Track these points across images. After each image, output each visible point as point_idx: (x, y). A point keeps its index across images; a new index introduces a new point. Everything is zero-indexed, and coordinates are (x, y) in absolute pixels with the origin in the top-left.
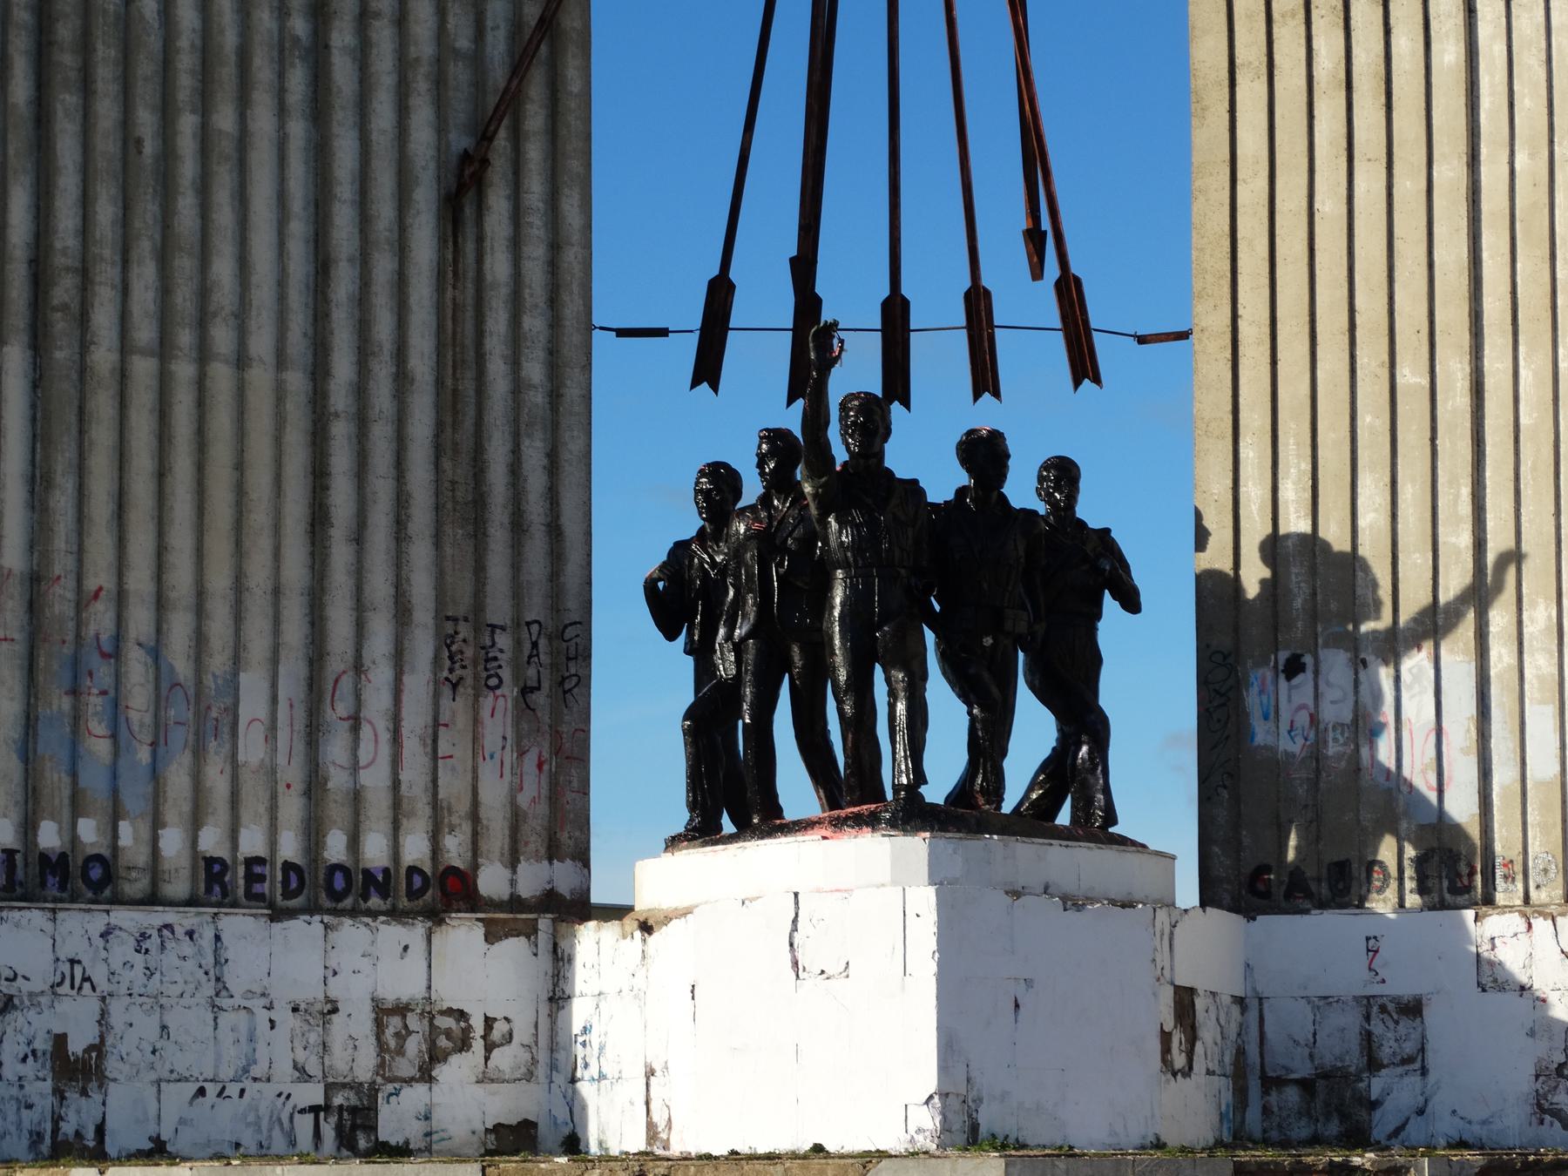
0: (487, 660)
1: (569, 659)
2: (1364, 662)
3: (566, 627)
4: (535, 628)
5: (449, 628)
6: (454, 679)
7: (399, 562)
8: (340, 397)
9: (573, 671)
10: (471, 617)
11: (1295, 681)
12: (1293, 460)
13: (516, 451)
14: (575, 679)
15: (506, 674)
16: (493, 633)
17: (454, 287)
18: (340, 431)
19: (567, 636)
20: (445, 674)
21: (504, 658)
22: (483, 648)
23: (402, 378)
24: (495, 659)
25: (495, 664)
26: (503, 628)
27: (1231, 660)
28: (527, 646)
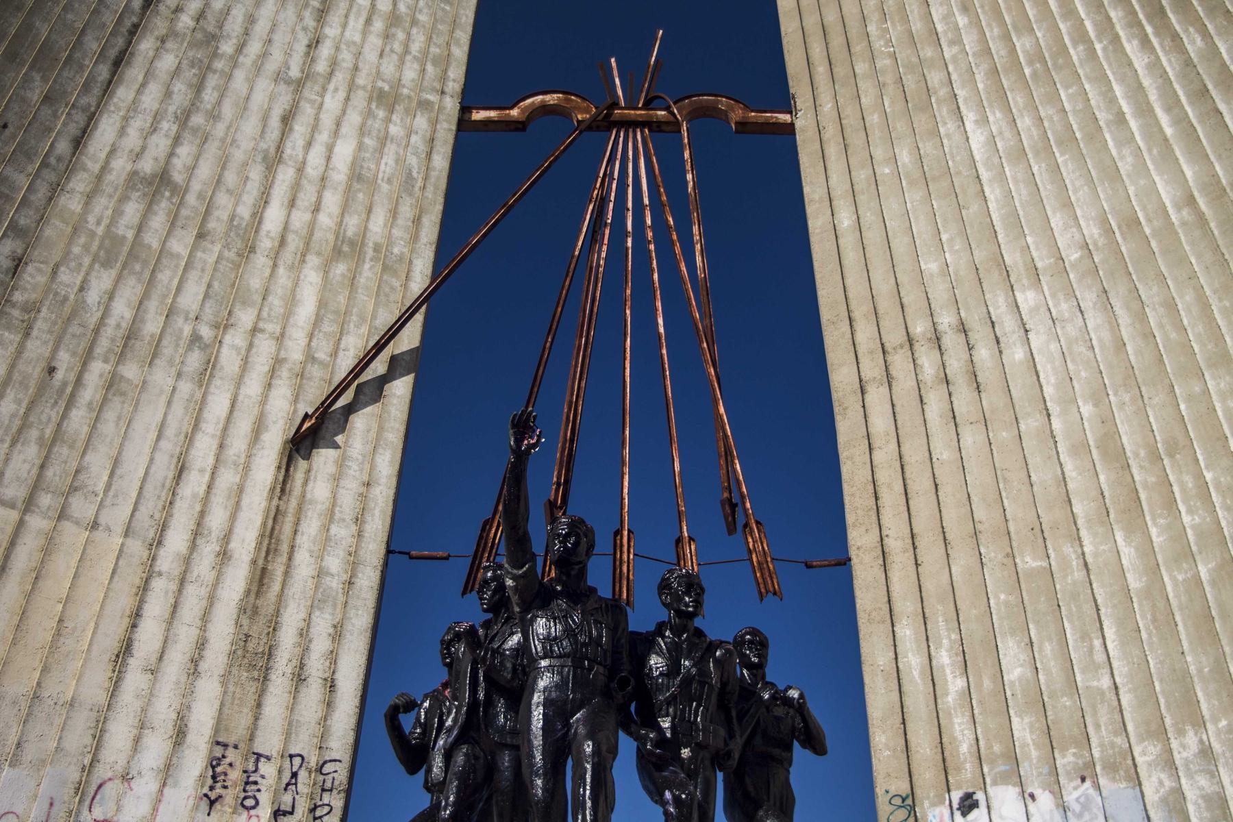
0: (247, 783)
1: (323, 790)
2: (1032, 796)
3: (325, 762)
4: (297, 761)
5: (218, 751)
6: (213, 796)
7: (188, 694)
8: (167, 561)
9: (326, 801)
10: (242, 745)
11: (971, 816)
12: (944, 633)
13: (308, 621)
14: (327, 809)
15: (265, 798)
16: (257, 761)
17: (280, 499)
18: (161, 588)
19: (325, 770)
20: (206, 790)
21: (263, 785)
22: (245, 772)
23: (224, 556)
24: (256, 783)
25: (254, 787)
26: (268, 758)
27: (909, 801)
28: (287, 776)
